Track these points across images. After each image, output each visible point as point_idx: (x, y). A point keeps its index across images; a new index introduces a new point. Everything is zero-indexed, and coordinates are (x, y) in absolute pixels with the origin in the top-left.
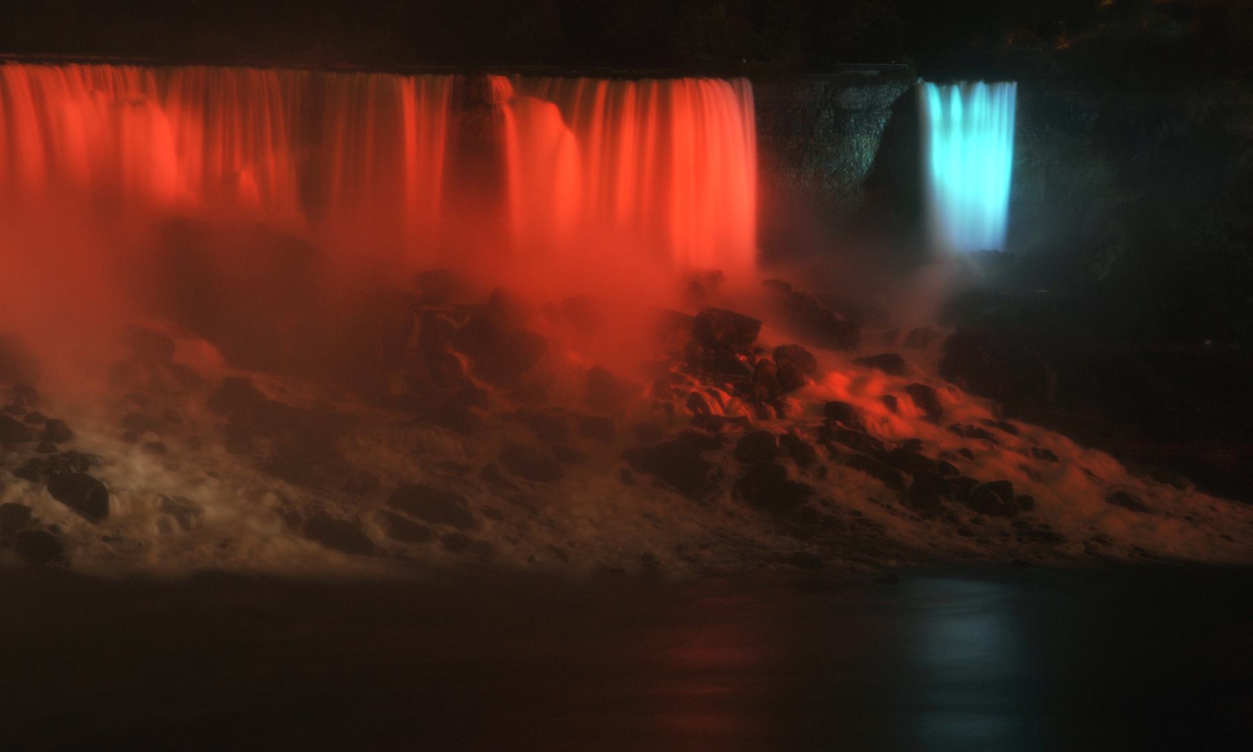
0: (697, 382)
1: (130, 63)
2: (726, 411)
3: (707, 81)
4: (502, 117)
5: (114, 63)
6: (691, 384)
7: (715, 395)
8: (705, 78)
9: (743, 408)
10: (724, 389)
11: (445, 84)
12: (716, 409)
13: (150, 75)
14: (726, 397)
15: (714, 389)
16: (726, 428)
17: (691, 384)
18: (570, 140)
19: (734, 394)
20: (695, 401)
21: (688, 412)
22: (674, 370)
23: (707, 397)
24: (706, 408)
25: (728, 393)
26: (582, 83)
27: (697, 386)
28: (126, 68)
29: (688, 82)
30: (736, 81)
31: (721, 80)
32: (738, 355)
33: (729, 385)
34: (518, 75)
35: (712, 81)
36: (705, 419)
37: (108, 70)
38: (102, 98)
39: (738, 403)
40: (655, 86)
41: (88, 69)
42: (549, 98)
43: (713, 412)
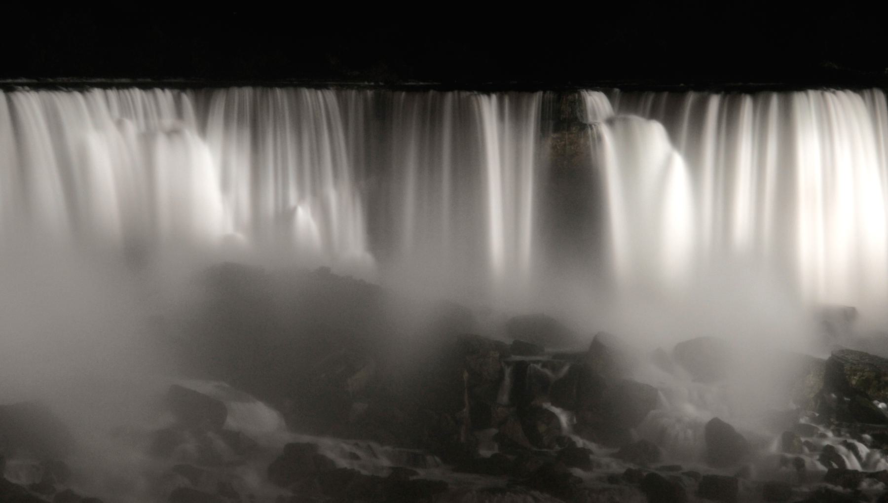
0: (830, 434)
1: (163, 87)
2: (864, 465)
3: (834, 93)
4: (600, 138)
5: (144, 87)
6: (824, 436)
7: (852, 448)
8: (832, 90)
9: (883, 461)
10: (862, 440)
11: (534, 104)
12: (853, 464)
13: (187, 100)
14: (863, 450)
15: (850, 441)
16: (865, 484)
17: (824, 436)
18: (679, 163)
19: (872, 446)
20: (829, 455)
21: (822, 468)
22: (803, 421)
23: (843, 450)
24: (842, 463)
25: (866, 445)
26: (691, 98)
27: (830, 439)
28: (158, 91)
29: (813, 95)
30: (867, 93)
31: (850, 93)
32: (876, 402)
33: (867, 436)
34: (617, 90)
35: (840, 93)
36: (841, 474)
37: (137, 94)
38: (131, 127)
39: (877, 455)
40: (775, 100)
41: (112, 94)
42: (653, 115)
43: (849, 466)
